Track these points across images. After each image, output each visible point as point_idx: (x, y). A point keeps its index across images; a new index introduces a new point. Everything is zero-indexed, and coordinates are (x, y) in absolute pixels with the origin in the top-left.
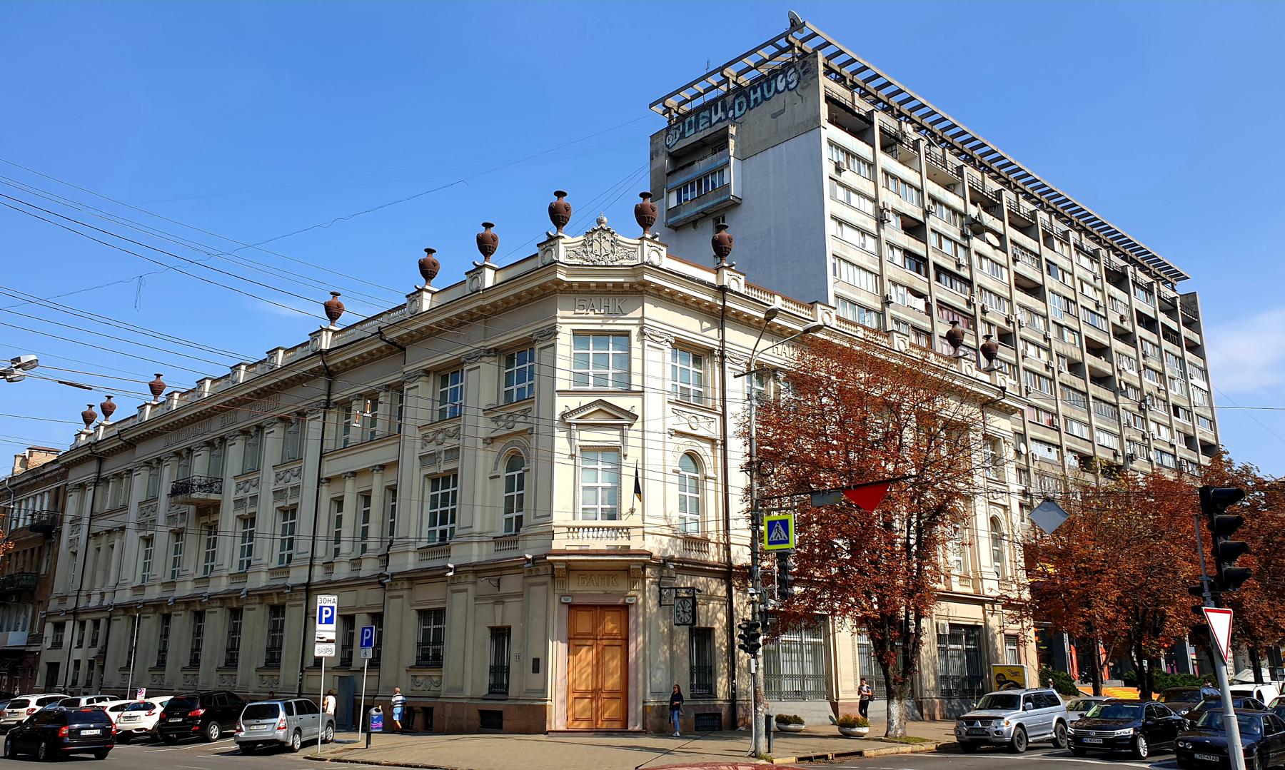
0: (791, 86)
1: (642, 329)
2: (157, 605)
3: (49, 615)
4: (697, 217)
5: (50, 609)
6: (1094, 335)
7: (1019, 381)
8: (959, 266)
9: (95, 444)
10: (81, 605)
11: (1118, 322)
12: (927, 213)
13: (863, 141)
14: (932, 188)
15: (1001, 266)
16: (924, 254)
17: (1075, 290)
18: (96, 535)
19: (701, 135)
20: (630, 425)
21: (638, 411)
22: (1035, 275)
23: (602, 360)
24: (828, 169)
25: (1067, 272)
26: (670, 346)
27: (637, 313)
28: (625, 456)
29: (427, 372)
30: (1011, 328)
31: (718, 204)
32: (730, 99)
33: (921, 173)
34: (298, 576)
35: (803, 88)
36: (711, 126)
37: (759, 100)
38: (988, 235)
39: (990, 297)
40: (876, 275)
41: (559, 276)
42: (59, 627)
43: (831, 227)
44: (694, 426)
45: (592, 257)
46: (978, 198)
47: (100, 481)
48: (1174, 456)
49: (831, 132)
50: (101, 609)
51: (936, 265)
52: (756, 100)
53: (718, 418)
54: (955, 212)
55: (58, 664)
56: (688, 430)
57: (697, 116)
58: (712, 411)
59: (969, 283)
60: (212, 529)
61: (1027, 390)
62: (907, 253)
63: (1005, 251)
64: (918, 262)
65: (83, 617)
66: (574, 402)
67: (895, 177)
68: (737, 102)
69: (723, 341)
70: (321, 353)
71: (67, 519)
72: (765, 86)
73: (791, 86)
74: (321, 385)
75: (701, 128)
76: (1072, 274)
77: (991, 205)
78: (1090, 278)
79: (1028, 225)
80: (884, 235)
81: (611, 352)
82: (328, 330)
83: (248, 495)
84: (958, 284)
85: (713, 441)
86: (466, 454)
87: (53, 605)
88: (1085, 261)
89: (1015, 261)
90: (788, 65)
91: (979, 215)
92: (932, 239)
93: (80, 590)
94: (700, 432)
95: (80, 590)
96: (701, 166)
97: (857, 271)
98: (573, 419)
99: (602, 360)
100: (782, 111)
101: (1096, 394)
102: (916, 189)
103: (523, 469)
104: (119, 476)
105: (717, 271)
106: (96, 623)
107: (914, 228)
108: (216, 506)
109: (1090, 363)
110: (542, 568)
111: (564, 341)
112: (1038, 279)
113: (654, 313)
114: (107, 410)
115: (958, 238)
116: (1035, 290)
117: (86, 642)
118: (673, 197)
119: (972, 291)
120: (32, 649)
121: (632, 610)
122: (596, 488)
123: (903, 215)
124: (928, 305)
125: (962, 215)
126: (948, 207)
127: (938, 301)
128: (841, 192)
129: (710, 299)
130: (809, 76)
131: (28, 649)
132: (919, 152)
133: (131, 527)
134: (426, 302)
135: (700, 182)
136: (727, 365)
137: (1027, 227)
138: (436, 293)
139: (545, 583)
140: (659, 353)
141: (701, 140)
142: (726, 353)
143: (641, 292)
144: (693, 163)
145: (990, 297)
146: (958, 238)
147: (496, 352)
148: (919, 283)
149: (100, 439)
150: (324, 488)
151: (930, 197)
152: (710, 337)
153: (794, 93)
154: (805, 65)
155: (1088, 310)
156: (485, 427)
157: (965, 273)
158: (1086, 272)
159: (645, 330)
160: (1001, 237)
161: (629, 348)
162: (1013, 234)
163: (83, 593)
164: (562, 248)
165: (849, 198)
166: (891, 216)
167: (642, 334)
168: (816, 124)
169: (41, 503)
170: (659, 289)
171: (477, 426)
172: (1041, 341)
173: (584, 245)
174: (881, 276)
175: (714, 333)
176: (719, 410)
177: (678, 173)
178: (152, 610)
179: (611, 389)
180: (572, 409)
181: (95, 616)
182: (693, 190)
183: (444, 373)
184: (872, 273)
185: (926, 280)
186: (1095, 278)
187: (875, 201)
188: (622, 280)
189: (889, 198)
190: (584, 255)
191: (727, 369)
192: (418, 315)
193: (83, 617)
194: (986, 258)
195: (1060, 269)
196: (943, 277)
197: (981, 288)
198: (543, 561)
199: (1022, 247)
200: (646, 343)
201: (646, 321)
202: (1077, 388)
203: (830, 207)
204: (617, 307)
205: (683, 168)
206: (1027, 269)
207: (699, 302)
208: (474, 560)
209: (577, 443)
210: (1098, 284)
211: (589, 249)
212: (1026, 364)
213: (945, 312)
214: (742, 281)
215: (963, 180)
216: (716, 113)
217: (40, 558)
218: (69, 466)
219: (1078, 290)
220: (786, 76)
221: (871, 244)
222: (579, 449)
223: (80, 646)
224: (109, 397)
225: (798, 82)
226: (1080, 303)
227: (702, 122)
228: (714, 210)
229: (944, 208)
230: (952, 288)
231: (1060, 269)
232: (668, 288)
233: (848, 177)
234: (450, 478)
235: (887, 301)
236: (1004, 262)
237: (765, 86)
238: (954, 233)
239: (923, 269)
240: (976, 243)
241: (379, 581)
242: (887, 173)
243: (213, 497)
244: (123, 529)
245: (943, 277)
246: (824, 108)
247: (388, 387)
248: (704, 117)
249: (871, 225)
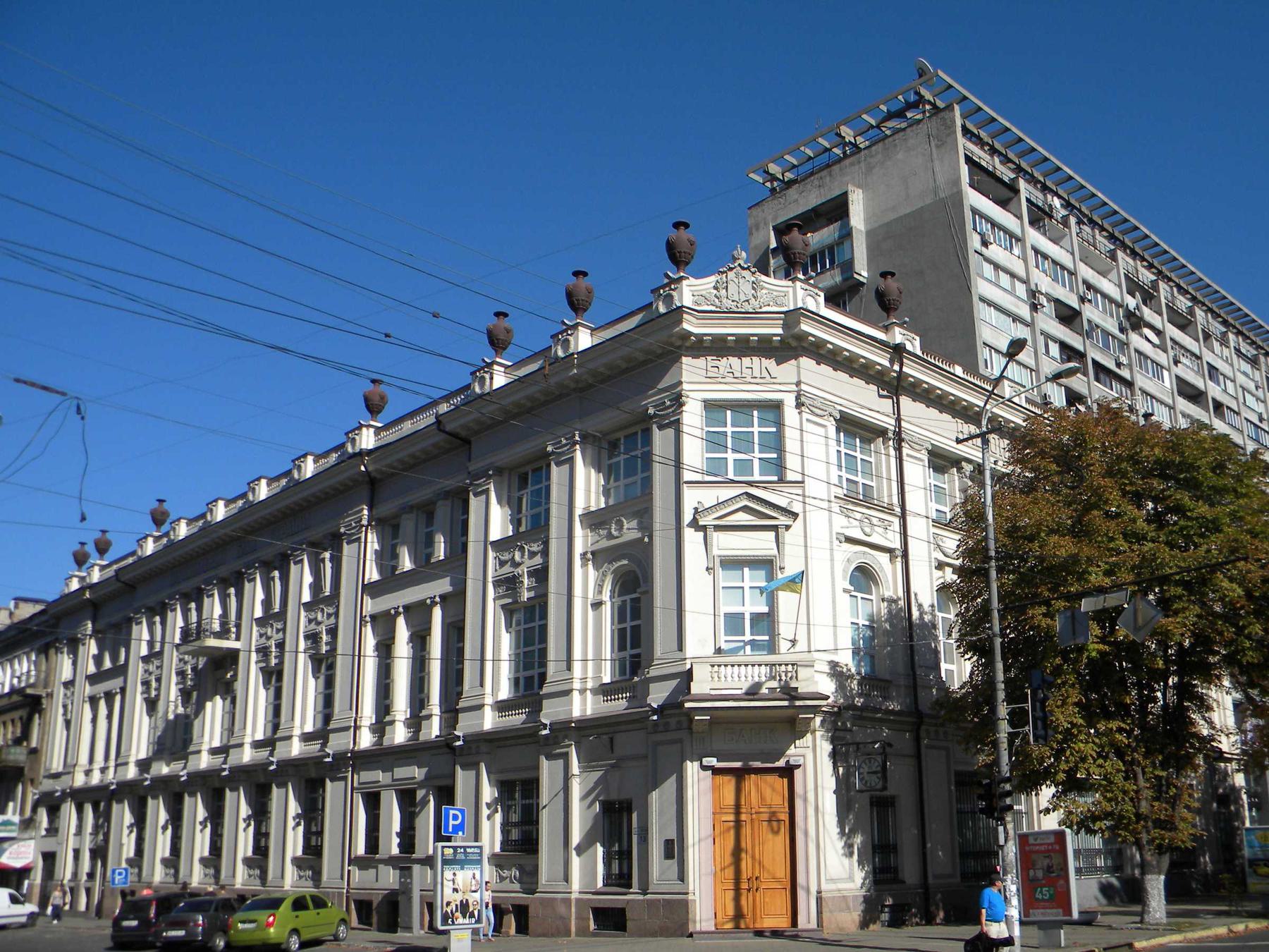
1: (798, 398)
8: (1119, 365)
13: (1004, 209)
14: (1085, 272)
15: (1162, 367)
16: (1081, 348)
17: (1236, 399)
20: (788, 527)
21: (797, 508)
23: (744, 442)
25: (1228, 378)
26: (834, 423)
28: (782, 568)
33: (1072, 254)
38: (1147, 331)
41: (685, 326)
44: (867, 530)
46: (1133, 286)
51: (1095, 363)
53: (896, 521)
54: (1112, 301)
56: (857, 534)
58: (889, 510)
62: (1064, 346)
63: (1165, 351)
66: (708, 496)
67: (1045, 257)
69: (899, 420)
76: (1233, 381)
78: (1252, 386)
79: (1187, 322)
81: (756, 429)
82: (369, 426)
85: (890, 551)
88: (1246, 367)
89: (1176, 362)
91: (1138, 307)
94: (875, 539)
99: (744, 442)
103: (638, 590)
105: (886, 329)
107: (1068, 316)
108: (231, 658)
110: (673, 721)
111: (692, 416)
114: (102, 548)
121: (798, 774)
123: (1058, 302)
125: (1119, 305)
128: (988, 270)
136: (905, 451)
137: (1184, 324)
138: (509, 366)
139: (681, 741)
140: (821, 431)
142: (903, 436)
151: (1085, 282)
155: (1251, 422)
156: (582, 540)
157: (1125, 373)
159: (803, 399)
160: (1159, 333)
161: (780, 424)
162: (1172, 331)
165: (998, 277)
166: (1043, 300)
167: (799, 405)
170: (820, 343)
173: (716, 288)
174: (1037, 371)
175: (887, 405)
176: (898, 510)
179: (757, 477)
180: (706, 507)
183: (522, 470)
184: (1026, 367)
185: (1085, 379)
186: (1257, 388)
187: (1025, 282)
190: (716, 300)
191: (905, 458)
195: (1222, 374)
196: (1102, 376)
197: (1144, 392)
198: (677, 711)
199: (1182, 347)
200: (805, 416)
201: (803, 387)
204: (764, 370)
207: (869, 365)
208: (576, 713)
209: (716, 552)
210: (1260, 393)
214: (917, 343)
215: (1118, 266)
219: (1241, 400)
222: (717, 561)
226: (1244, 414)
229: (1099, 295)
230: (1112, 390)
231: (1222, 374)
232: (831, 343)
233: (995, 252)
234: (538, 608)
236: (1165, 363)
238: (1111, 325)
240: (1134, 338)
241: (445, 745)
242: (1037, 251)
247: (447, 495)
249: (1024, 311)
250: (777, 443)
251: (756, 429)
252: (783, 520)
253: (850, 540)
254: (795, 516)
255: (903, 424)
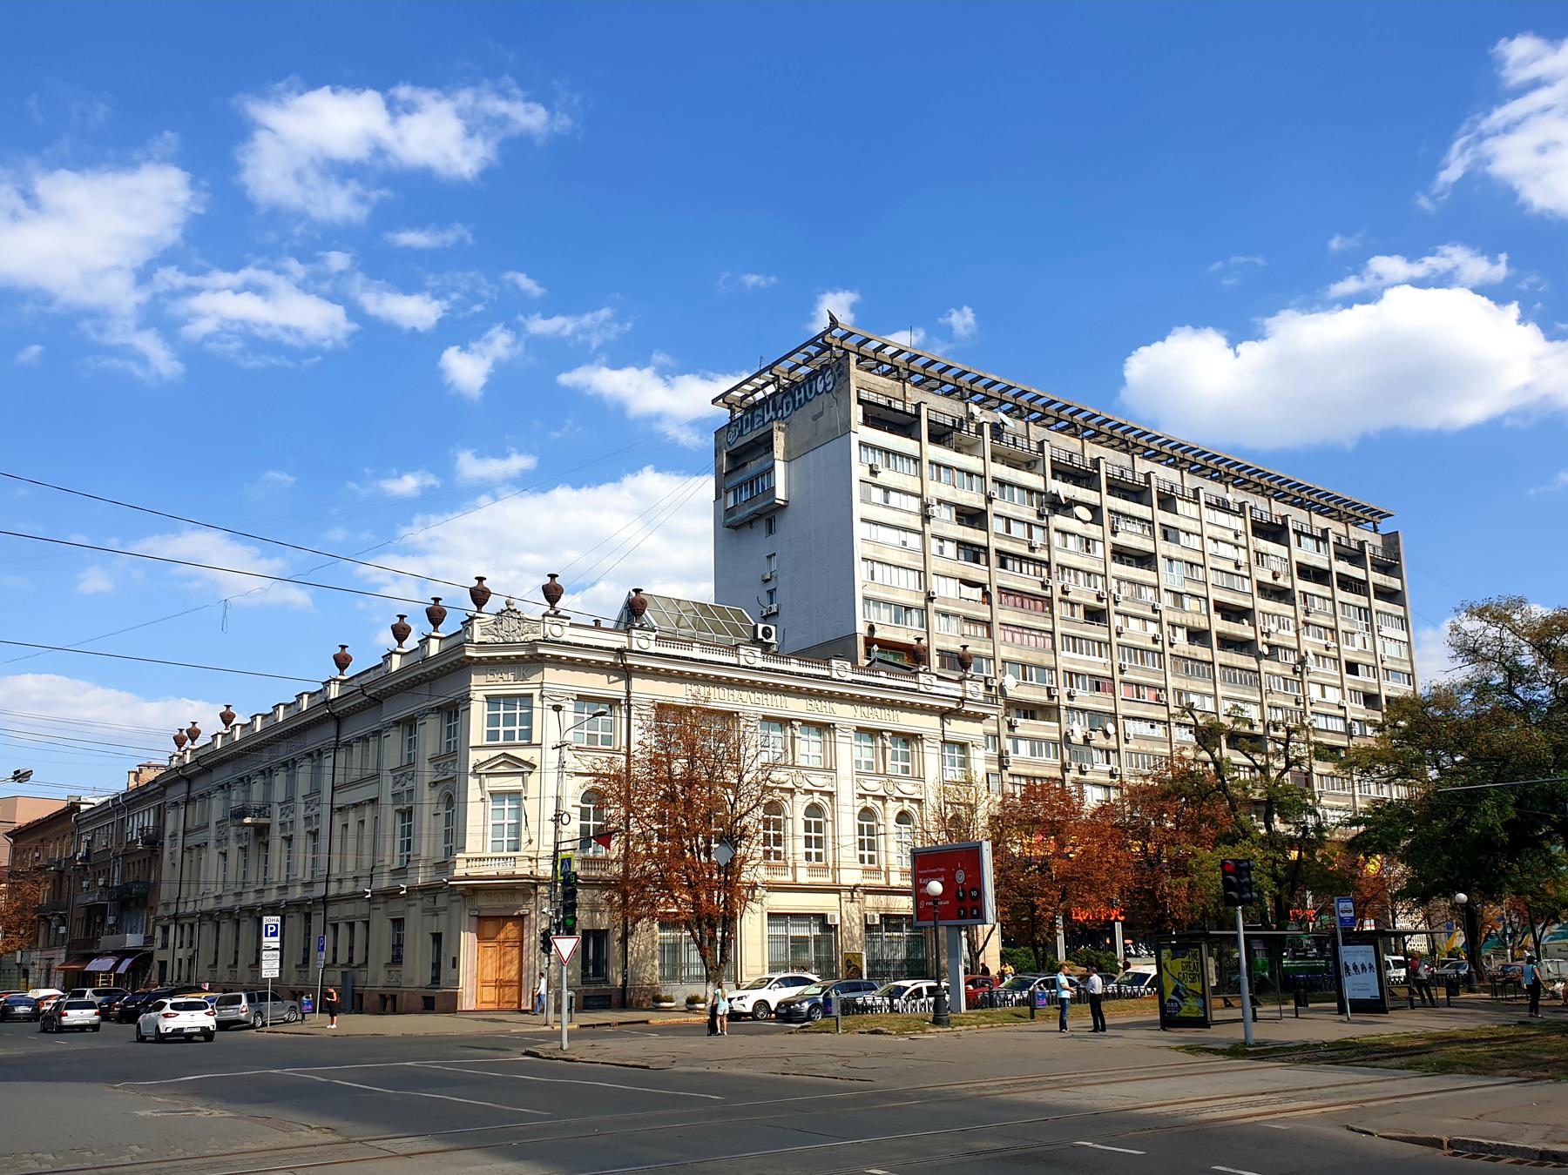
0: (829, 388)
2: (230, 912)
3: (157, 920)
4: (752, 517)
5: (159, 914)
6: (1228, 598)
7: (1112, 659)
8: (1032, 549)
9: (182, 768)
10: (181, 911)
11: (1269, 580)
12: (989, 499)
18: (189, 848)
19: (754, 435)
20: (530, 773)
22: (1145, 544)
24: (859, 471)
27: (536, 678)
29: (397, 723)
30: (1104, 604)
31: (767, 505)
32: (779, 398)
33: (984, 458)
34: (319, 891)
35: (838, 391)
36: (764, 425)
37: (803, 401)
39: (1076, 576)
40: (920, 572)
41: (468, 654)
42: (166, 930)
43: (860, 530)
45: (502, 633)
46: (1064, 472)
47: (188, 801)
48: (1345, 719)
49: (863, 433)
50: (192, 915)
51: (997, 551)
52: (800, 399)
54: (1030, 491)
55: (166, 962)
57: (753, 414)
59: (1047, 564)
60: (267, 845)
61: (1120, 668)
62: (961, 544)
64: (973, 552)
65: (182, 921)
66: (484, 756)
68: (785, 401)
69: (628, 692)
70: (327, 702)
71: (168, 834)
72: (807, 386)
73: (829, 388)
74: (331, 729)
75: (756, 426)
77: (1084, 477)
80: (928, 530)
83: (288, 819)
84: (1031, 567)
86: (417, 795)
87: (161, 911)
90: (825, 367)
92: (997, 525)
93: (179, 898)
95: (179, 898)
96: (753, 467)
97: (894, 570)
98: (482, 770)
99: (510, 720)
100: (821, 414)
101: (1223, 661)
102: (978, 475)
104: (202, 796)
106: (192, 926)
109: (1221, 629)
112: (1148, 546)
113: (551, 675)
115: (1034, 519)
116: (1146, 560)
117: (185, 944)
118: (731, 496)
119: (1049, 573)
120: (148, 949)
122: (503, 825)
123: (956, 505)
124: (986, 594)
126: (1020, 487)
127: (999, 587)
129: (612, 660)
130: (843, 378)
131: (144, 949)
132: (983, 435)
133: (212, 843)
134: (396, 663)
135: (752, 482)
136: (633, 712)
141: (753, 441)
143: (540, 661)
144: (746, 464)
145: (1076, 576)
146: (1034, 519)
147: (439, 709)
148: (977, 572)
149: (188, 762)
150: (336, 818)
152: (617, 689)
153: (830, 395)
154: (839, 371)
158: (1223, 530)
161: (531, 707)
163: (182, 900)
164: (476, 626)
167: (542, 697)
168: (847, 429)
169: (148, 820)
171: (427, 773)
172: (1150, 614)
173: (495, 623)
177: (734, 474)
178: (247, 914)
179: (517, 741)
181: (191, 921)
182: (746, 491)
185: (987, 568)
186: (1236, 536)
187: (920, 496)
188: (523, 653)
189: (937, 489)
192: (390, 675)
193: (182, 921)
194: (1073, 534)
195: (1183, 531)
197: (1063, 567)
202: (1199, 658)
203: (859, 510)
205: (737, 469)
206: (1132, 538)
209: (487, 789)
210: (1242, 541)
211: (499, 626)
212: (1122, 640)
213: (1011, 598)
215: (1044, 457)
216: (768, 412)
217: (150, 868)
218: (166, 785)
220: (824, 378)
221: (914, 541)
223: (181, 947)
224: (228, 707)
225: (834, 384)
227: (757, 420)
228: (765, 511)
233: (886, 477)
235: (930, 598)
237: (807, 386)
238: (1029, 514)
239: (983, 558)
240: (1059, 521)
243: (263, 821)
244: (206, 844)
245: (1009, 563)
246: (857, 412)
248: (758, 416)
249: (916, 523)
250: (527, 719)
251: (518, 711)
252: (526, 769)
253: (577, 774)
254: (535, 766)
255: (632, 695)
